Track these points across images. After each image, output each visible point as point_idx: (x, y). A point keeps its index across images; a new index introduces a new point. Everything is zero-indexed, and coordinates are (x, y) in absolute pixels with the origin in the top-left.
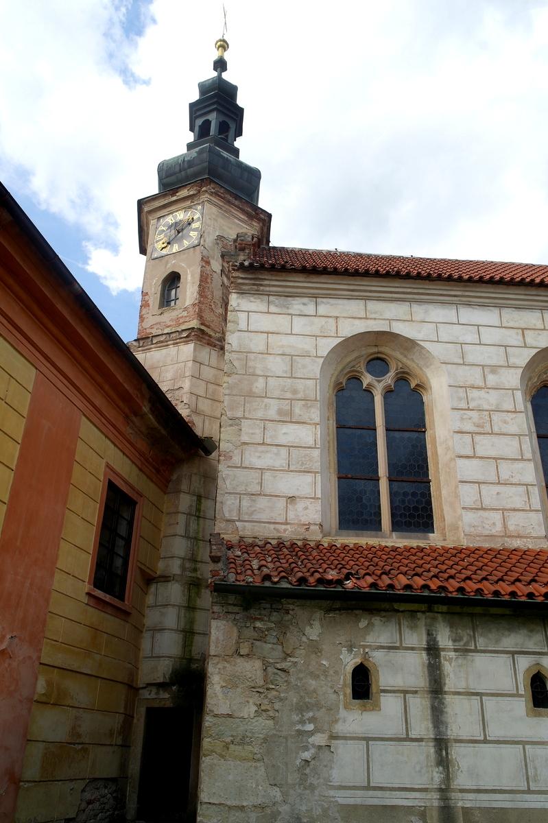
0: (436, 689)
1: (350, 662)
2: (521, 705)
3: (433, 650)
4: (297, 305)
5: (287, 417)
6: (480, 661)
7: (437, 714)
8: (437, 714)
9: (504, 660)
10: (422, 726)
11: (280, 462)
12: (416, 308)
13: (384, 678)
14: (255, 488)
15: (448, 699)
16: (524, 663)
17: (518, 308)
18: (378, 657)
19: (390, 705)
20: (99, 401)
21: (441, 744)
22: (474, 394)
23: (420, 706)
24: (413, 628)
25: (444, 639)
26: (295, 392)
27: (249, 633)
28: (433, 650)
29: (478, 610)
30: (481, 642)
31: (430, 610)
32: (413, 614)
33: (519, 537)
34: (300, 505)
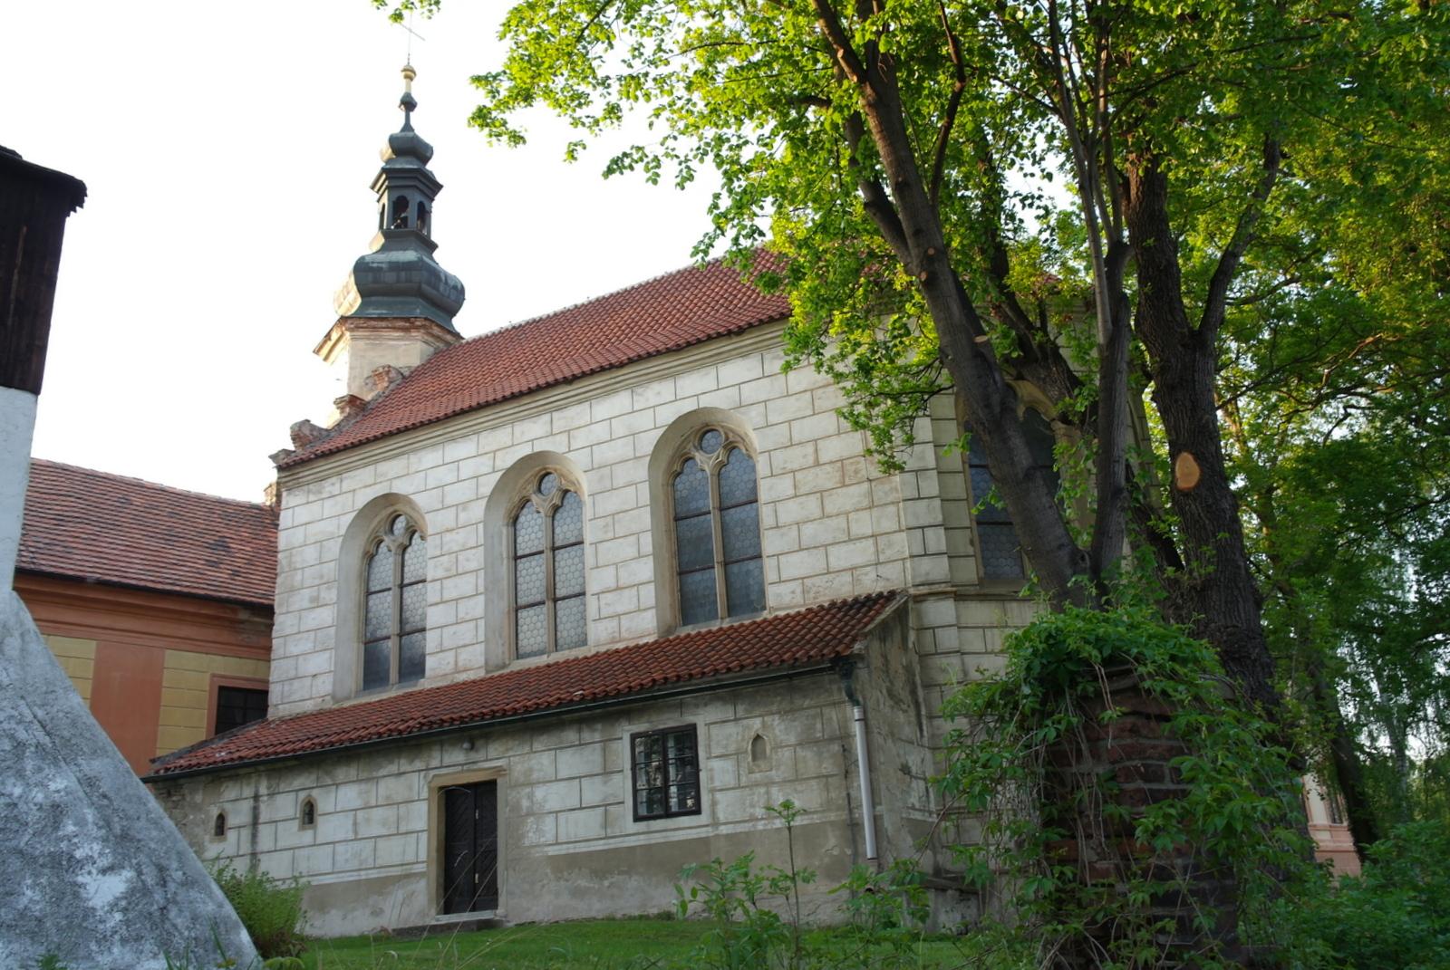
0: (255, 822)
1: (215, 812)
2: (296, 824)
3: (256, 797)
4: (330, 487)
5: (317, 603)
6: (280, 799)
7: (254, 836)
8: (254, 836)
9: (292, 796)
10: (246, 848)
11: (308, 646)
12: (413, 458)
13: (231, 821)
14: (292, 674)
15: (261, 827)
16: (302, 795)
17: (494, 428)
18: (228, 806)
19: (231, 836)
20: (186, 630)
21: (254, 855)
22: (448, 537)
23: (246, 833)
24: (248, 784)
25: (263, 790)
26: (322, 577)
27: (170, 804)
28: (256, 797)
29: (280, 765)
30: (282, 787)
31: (257, 771)
32: (248, 775)
33: (465, 670)
34: (320, 679)
